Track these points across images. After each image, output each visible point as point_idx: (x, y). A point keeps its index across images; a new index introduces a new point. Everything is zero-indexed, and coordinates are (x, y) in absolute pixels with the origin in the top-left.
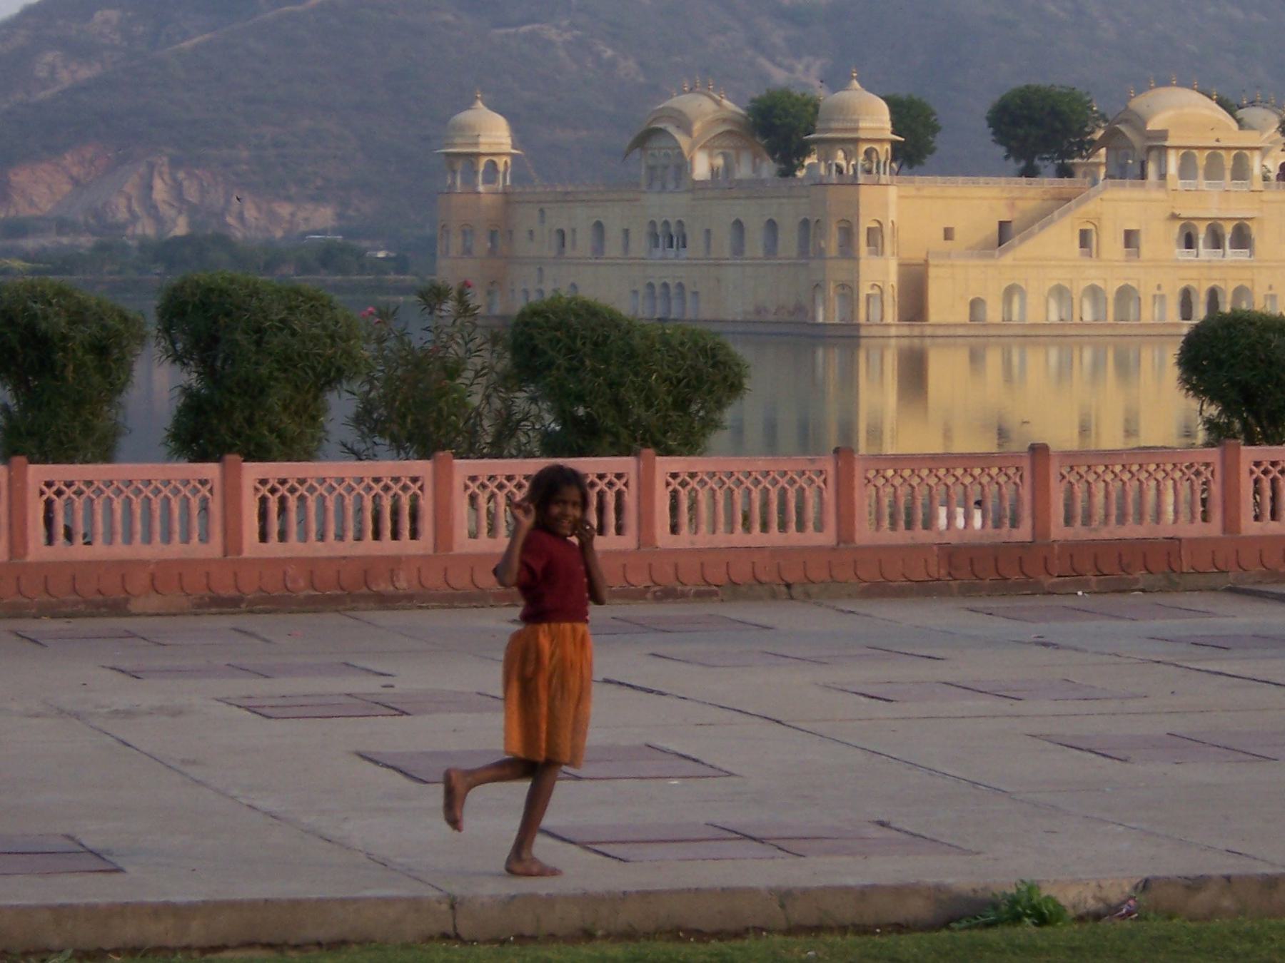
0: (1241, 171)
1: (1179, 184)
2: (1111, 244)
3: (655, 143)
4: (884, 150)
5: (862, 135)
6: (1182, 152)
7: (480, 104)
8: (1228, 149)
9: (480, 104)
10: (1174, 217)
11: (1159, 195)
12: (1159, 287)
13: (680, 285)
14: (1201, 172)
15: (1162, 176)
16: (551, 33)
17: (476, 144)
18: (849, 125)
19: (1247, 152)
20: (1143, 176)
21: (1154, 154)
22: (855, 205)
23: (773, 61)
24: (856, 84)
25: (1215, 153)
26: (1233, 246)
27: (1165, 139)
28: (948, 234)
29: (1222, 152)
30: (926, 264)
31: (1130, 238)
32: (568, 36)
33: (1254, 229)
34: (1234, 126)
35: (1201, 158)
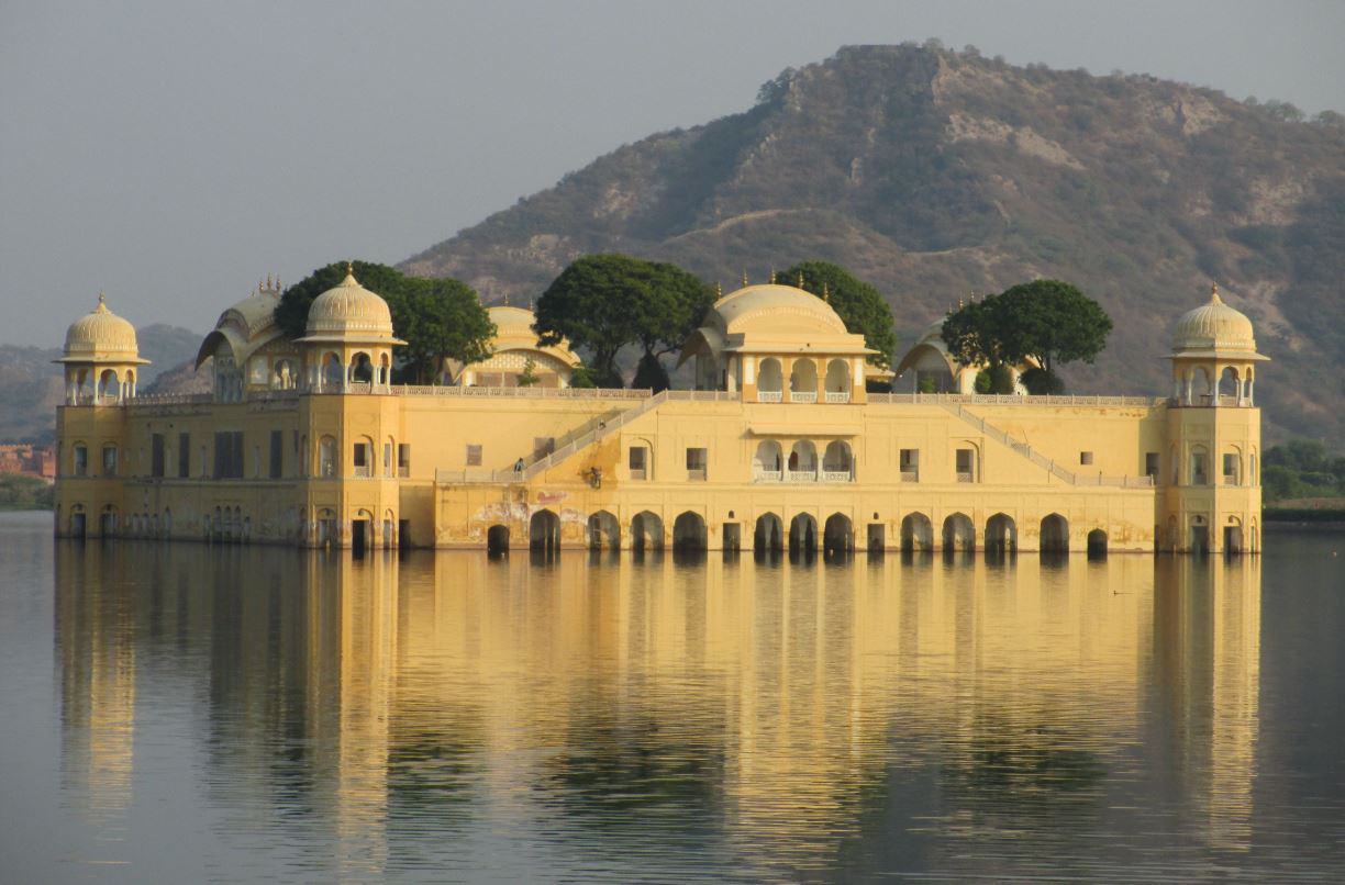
0: (839, 381)
1: (760, 396)
3: (222, 351)
4: (389, 352)
5: (347, 338)
6: (760, 360)
8: (822, 355)
10: (750, 435)
11: (735, 407)
12: (731, 514)
13: (238, 509)
14: (788, 384)
15: (739, 386)
16: (979, 256)
17: (92, 352)
18: (335, 327)
19: (848, 360)
20: (724, 387)
21: (733, 361)
22: (338, 416)
24: (351, 280)
25: (804, 359)
26: (827, 467)
27: (741, 343)
28: (474, 456)
29: (815, 361)
30: (434, 483)
31: (695, 459)
32: (996, 259)
33: (856, 449)
34: (842, 327)
35: (787, 367)
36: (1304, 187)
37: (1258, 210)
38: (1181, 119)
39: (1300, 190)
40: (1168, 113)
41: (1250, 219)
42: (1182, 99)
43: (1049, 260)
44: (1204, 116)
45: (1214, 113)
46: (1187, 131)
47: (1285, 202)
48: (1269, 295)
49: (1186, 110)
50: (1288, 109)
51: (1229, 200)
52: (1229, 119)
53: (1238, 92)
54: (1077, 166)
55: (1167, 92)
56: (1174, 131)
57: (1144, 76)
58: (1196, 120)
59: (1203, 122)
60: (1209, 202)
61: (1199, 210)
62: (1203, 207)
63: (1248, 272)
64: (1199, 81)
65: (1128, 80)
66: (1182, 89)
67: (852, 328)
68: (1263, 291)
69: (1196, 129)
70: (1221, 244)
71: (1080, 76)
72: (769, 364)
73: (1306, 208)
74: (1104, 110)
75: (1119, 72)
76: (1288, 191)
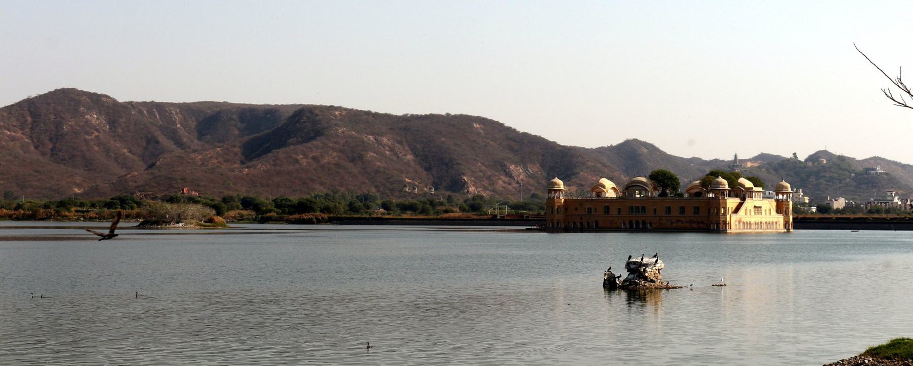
10: (755, 207)
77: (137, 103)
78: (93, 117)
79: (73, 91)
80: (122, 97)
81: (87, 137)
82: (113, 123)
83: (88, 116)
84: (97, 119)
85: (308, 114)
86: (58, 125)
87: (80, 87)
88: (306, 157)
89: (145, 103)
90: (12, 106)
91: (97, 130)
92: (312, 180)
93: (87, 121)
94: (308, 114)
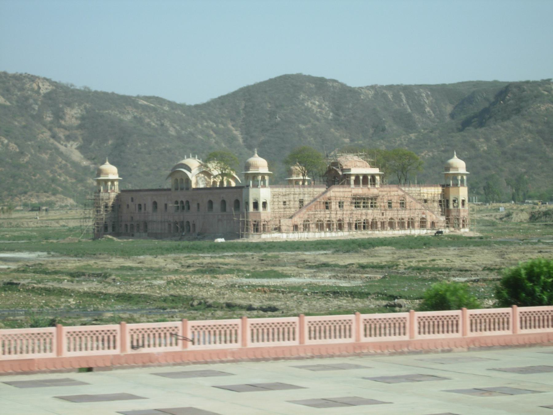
2: (334, 206)
7: (107, 163)
9: (107, 163)
11: (350, 190)
23: (59, 142)
25: (365, 176)
31: (341, 205)
36: (81, 110)
37: (67, 117)
38: (39, 88)
39: (80, 111)
40: (35, 86)
41: (65, 121)
42: (39, 81)
43: (7, 135)
44: (46, 87)
45: (49, 86)
46: (41, 92)
47: (75, 116)
48: (75, 146)
49: (41, 85)
50: (72, 85)
51: (58, 116)
52: (54, 88)
53: (55, 79)
54: (8, 103)
55: (33, 79)
56: (38, 92)
57: (26, 73)
58: (45, 88)
59: (46, 89)
60: (51, 115)
61: (48, 118)
62: (49, 117)
63: (68, 138)
64: (42, 75)
65: (21, 75)
66: (38, 78)
67: (373, 165)
68: (72, 145)
69: (45, 91)
70: (56, 130)
71: (5, 73)
72: (357, 176)
73: (83, 118)
74: (14, 85)
75: (17, 73)
76: (76, 112)
77: (382, 87)
78: (314, 104)
79: (299, 77)
80: (354, 80)
81: (302, 127)
82: (337, 109)
83: (309, 104)
84: (320, 106)
85: (515, 90)
86: (272, 114)
87: (306, 73)
88: (487, 140)
89: (390, 87)
90: (227, 96)
91: (318, 120)
92: (485, 168)
93: (307, 109)
94: (515, 90)
